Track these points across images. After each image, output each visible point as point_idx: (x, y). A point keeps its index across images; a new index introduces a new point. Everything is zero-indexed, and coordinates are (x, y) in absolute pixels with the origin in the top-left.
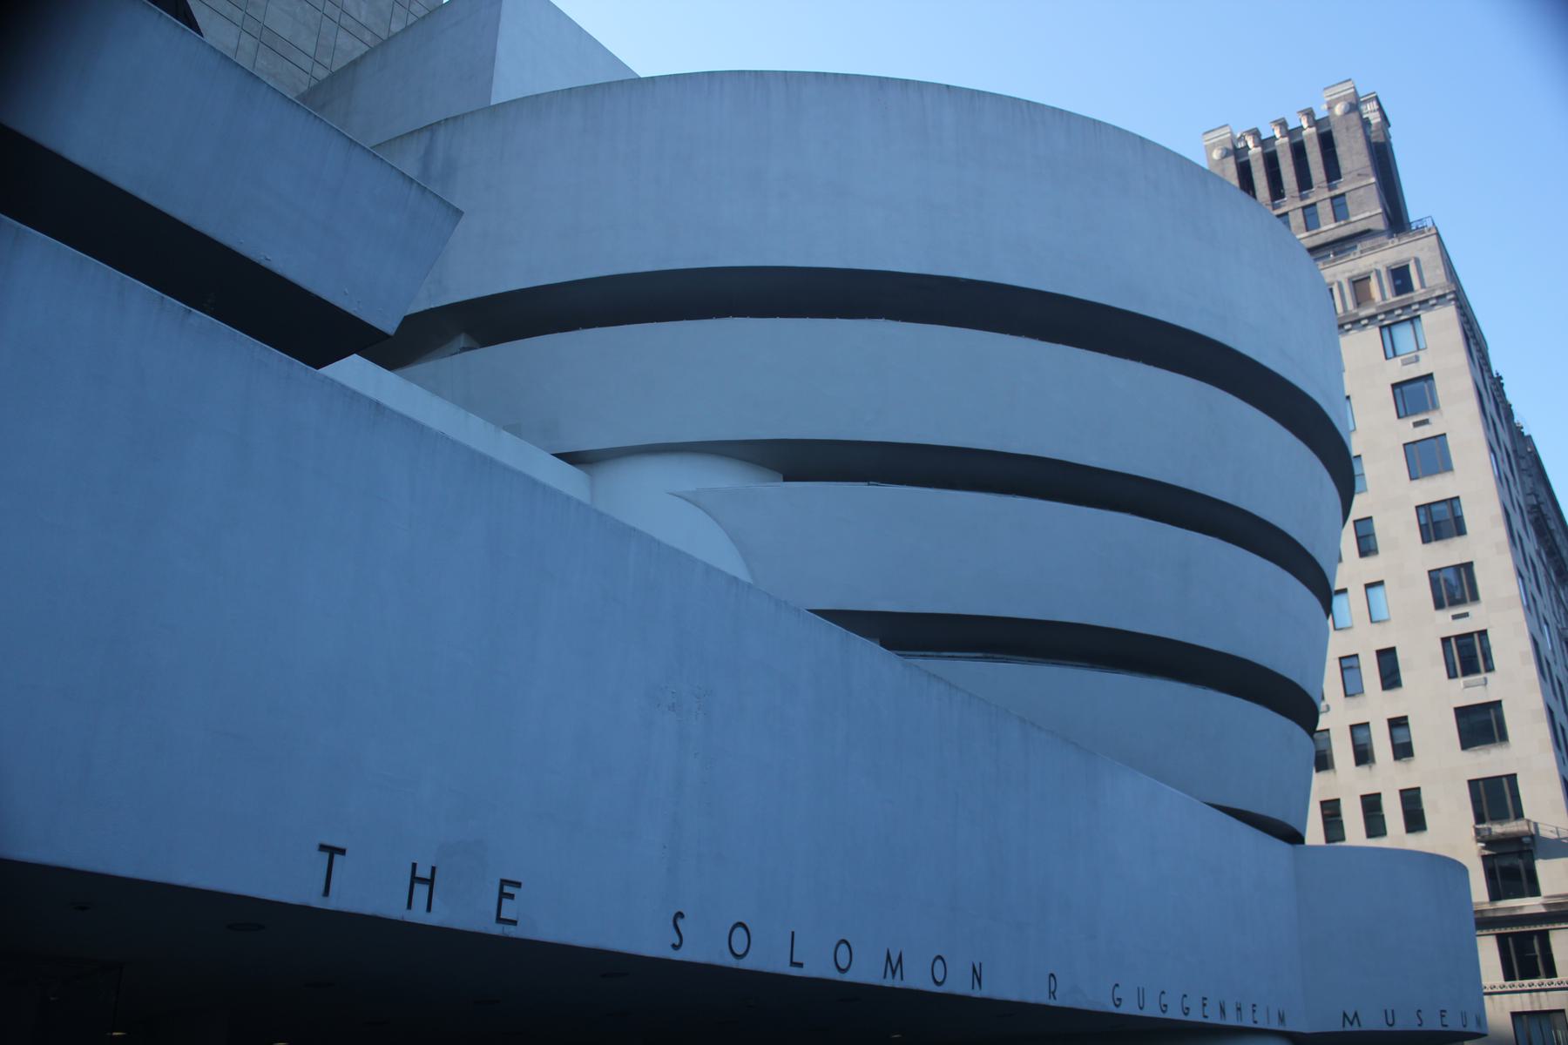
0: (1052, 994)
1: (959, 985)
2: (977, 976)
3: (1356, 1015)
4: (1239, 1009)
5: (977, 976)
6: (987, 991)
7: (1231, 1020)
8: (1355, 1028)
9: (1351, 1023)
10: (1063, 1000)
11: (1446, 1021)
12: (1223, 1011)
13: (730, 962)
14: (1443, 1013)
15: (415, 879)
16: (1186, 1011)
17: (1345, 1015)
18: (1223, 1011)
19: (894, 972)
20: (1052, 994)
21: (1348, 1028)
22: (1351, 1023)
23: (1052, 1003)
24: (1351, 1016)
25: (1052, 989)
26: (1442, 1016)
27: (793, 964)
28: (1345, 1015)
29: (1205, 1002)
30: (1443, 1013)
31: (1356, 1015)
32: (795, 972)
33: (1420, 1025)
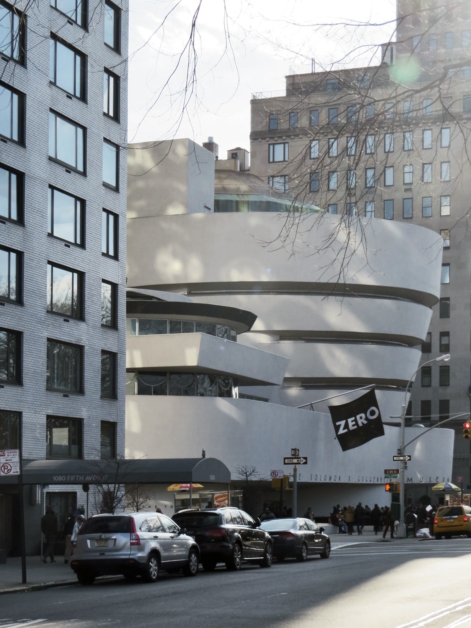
0: (349, 480)
3: (411, 479)
4: (381, 479)
7: (379, 482)
8: (411, 482)
9: (410, 481)
11: (438, 480)
14: (437, 478)
16: (370, 481)
17: (408, 479)
20: (349, 480)
21: (409, 482)
22: (410, 481)
24: (410, 479)
26: (437, 479)
28: (408, 479)
30: (437, 478)
31: (411, 479)
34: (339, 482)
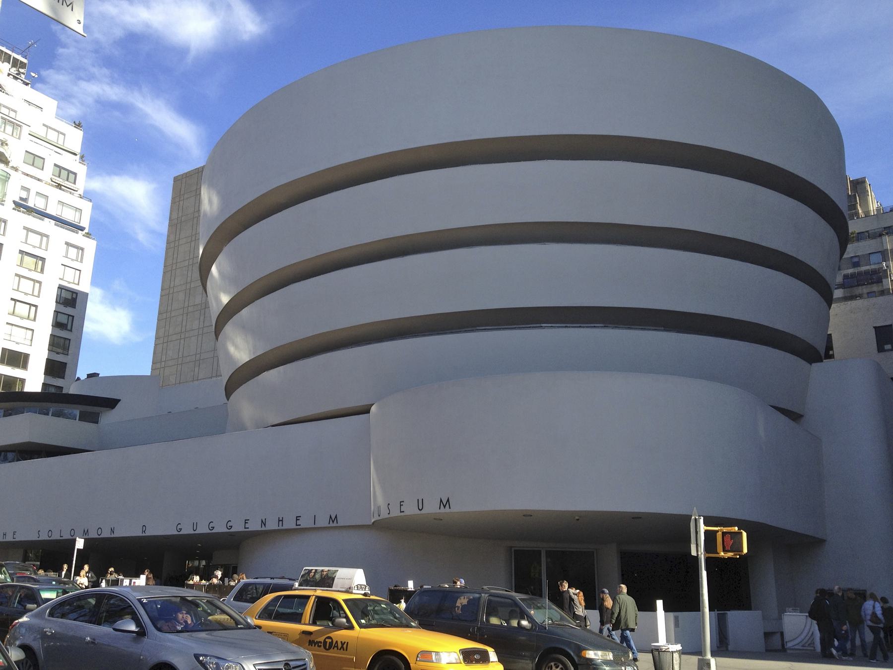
1: (106, 534)
2: (112, 531)
5: (112, 531)
6: (118, 534)
10: (150, 532)
12: (263, 523)
13: (48, 539)
15: (4, 535)
18: (263, 523)
19: (86, 535)
23: (144, 535)
25: (144, 530)
27: (61, 537)
29: (246, 521)
32: (61, 538)
33: (389, 514)
34: (112, 536)
